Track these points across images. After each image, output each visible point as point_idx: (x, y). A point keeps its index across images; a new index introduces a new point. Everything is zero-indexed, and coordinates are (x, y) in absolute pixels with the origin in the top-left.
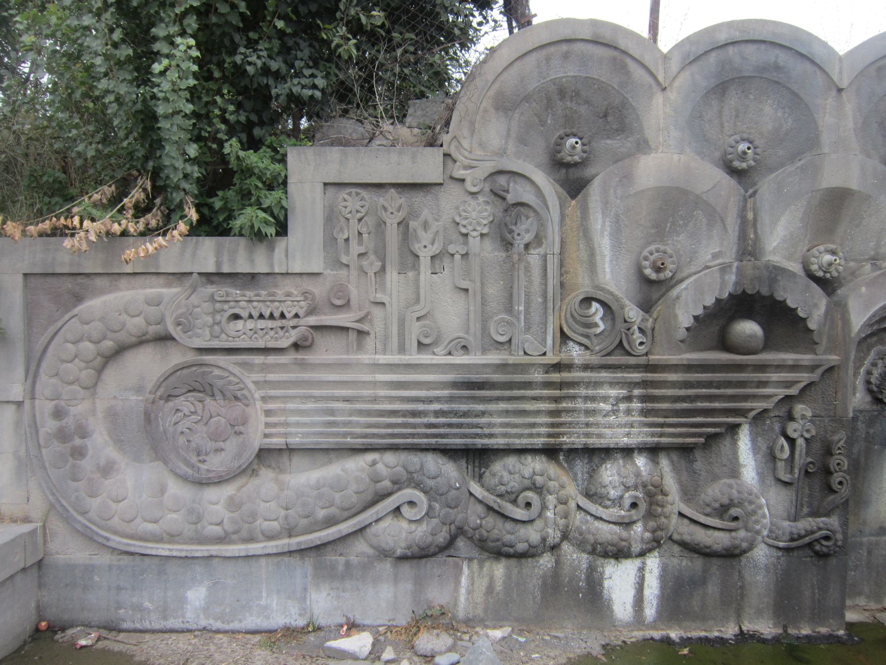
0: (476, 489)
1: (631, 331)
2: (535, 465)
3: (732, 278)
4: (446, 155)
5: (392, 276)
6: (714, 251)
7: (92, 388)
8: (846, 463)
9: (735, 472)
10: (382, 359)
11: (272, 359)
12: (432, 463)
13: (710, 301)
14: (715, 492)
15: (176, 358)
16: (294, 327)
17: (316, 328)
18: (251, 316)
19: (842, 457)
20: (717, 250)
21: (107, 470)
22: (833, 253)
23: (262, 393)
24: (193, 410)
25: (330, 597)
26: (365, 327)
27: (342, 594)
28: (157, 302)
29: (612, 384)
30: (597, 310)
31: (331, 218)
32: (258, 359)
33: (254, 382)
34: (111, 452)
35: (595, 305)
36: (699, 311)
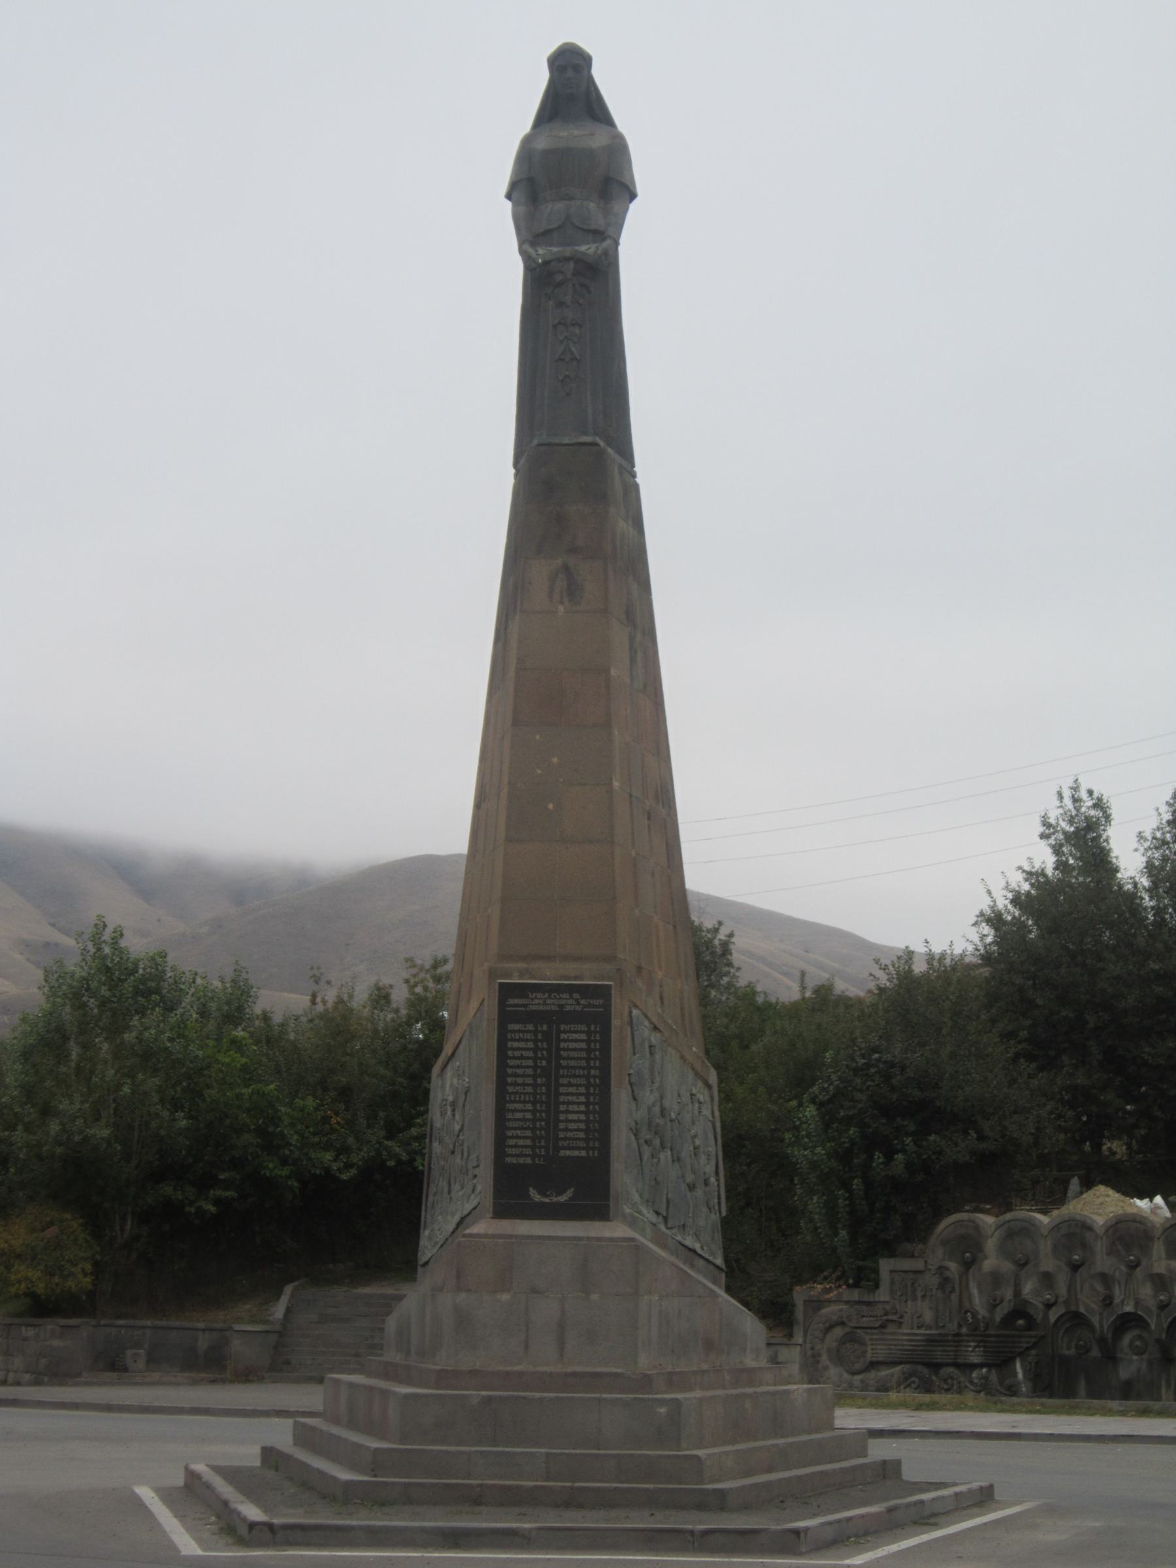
0: (934, 1378)
2: (951, 1369)
3: (1012, 1304)
4: (926, 1261)
5: (909, 1303)
7: (823, 1340)
9: (1015, 1375)
10: (906, 1331)
11: (874, 1331)
12: (920, 1368)
14: (1007, 1382)
15: (847, 1330)
17: (887, 1320)
21: (826, 1368)
22: (1050, 1294)
26: (901, 1320)
28: (841, 1310)
29: (973, 1341)
31: (892, 1282)
32: (869, 1331)
34: (828, 1363)
35: (969, 1314)
36: (1003, 1316)
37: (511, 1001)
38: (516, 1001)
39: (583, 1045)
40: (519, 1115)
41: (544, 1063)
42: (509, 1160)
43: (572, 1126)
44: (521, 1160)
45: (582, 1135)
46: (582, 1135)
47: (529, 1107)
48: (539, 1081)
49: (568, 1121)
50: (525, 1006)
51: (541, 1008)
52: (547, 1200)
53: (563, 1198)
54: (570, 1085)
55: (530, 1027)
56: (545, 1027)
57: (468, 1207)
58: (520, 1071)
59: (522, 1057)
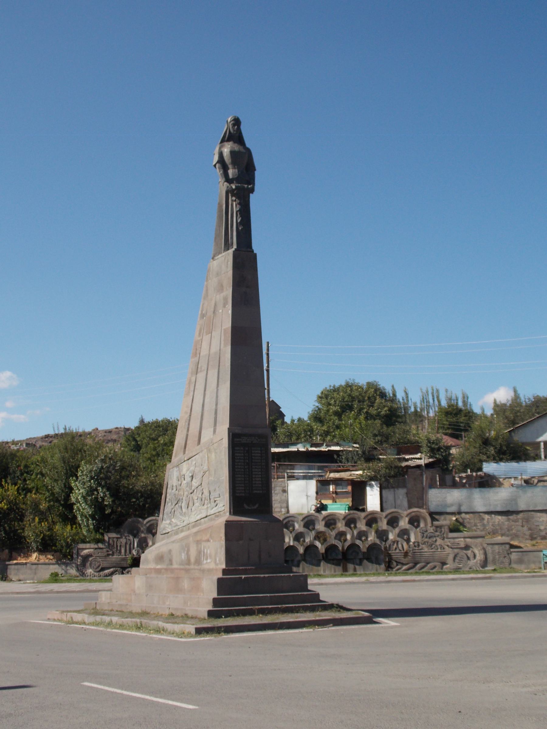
32: (101, 557)
37: (235, 440)
38: (238, 440)
39: (259, 455)
40: (239, 479)
41: (247, 461)
42: (238, 495)
43: (257, 482)
44: (241, 495)
45: (260, 485)
46: (260, 485)
47: (243, 476)
48: (246, 467)
49: (255, 480)
50: (240, 441)
51: (245, 442)
52: (250, 508)
53: (255, 507)
54: (256, 468)
55: (242, 448)
56: (247, 449)
57: (212, 512)
58: (239, 464)
59: (240, 459)
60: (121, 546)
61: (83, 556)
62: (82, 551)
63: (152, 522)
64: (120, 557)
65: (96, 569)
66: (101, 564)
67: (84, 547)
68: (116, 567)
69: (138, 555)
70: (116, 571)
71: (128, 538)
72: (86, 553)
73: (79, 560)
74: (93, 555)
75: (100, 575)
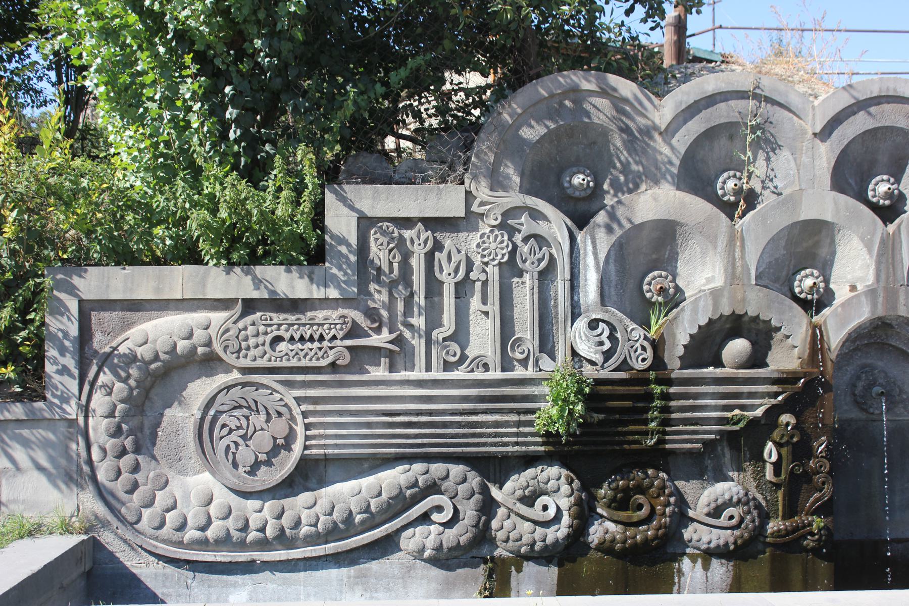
1: (634, 348)
4: (468, 193)
6: (707, 276)
8: (828, 466)
13: (703, 321)
16: (331, 348)
18: (292, 338)
19: (824, 460)
20: (710, 275)
23: (304, 407)
24: (239, 425)
25: (363, 597)
27: (375, 595)
30: (603, 330)
33: (295, 398)
36: (695, 331)
60: (463, 289)
61: (132, 359)
62: (126, 325)
63: (722, 113)
64: (458, 374)
65: (253, 470)
66: (300, 430)
67: (144, 293)
68: (429, 458)
69: (614, 361)
70: (433, 488)
71: (525, 224)
72: (162, 345)
73: (99, 401)
74: (230, 358)
75: (286, 521)
